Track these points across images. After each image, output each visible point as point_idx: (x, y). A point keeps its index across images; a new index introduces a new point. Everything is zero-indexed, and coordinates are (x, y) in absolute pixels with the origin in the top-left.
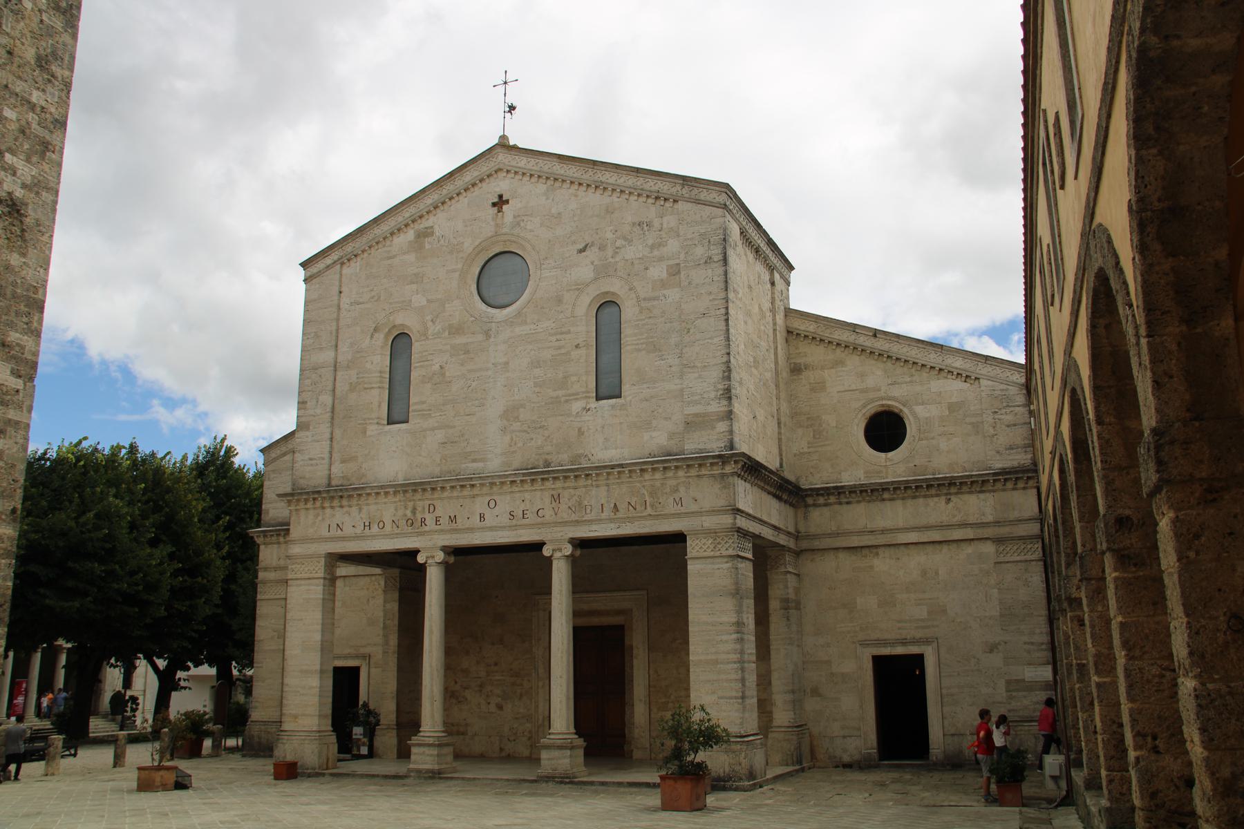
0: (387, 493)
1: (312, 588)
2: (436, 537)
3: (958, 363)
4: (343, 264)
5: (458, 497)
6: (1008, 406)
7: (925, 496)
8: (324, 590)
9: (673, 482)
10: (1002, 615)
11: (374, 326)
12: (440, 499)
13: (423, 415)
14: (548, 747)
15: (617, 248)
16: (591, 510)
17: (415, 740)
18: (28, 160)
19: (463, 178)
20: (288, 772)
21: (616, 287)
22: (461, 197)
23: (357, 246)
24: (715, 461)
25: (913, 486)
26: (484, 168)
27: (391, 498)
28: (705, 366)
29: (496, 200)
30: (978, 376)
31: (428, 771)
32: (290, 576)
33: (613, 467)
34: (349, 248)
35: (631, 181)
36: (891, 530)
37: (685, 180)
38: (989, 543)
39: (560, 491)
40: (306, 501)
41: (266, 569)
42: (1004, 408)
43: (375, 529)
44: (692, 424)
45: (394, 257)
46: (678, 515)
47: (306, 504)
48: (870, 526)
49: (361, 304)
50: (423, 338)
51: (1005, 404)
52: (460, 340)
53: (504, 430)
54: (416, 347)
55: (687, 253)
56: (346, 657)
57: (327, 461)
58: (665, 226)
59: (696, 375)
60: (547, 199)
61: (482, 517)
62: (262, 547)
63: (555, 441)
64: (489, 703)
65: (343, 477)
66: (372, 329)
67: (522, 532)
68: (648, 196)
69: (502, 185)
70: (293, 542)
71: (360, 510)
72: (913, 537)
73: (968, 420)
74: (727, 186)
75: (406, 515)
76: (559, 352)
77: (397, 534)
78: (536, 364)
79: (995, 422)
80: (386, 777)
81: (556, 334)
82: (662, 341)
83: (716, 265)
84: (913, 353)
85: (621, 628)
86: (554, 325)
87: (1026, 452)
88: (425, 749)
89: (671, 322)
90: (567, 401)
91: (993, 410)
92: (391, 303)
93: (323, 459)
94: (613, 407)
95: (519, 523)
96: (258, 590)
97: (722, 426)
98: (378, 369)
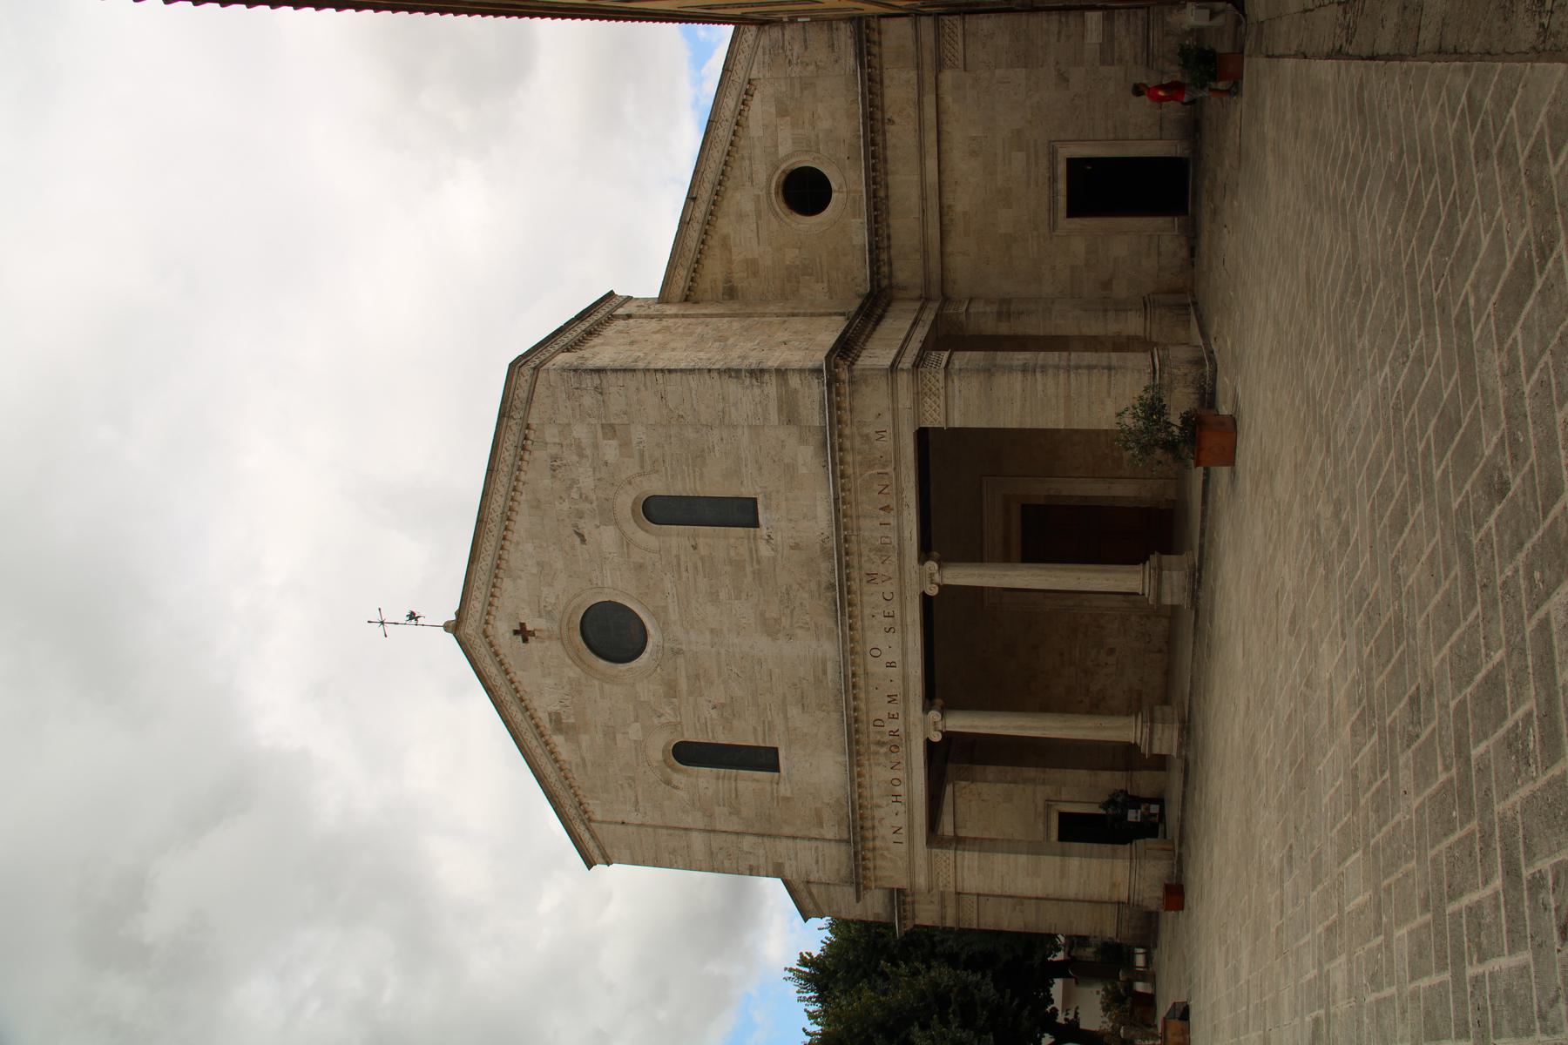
0: (860, 775)
1: (966, 863)
2: (912, 719)
3: (730, 103)
4: (590, 820)
5: (867, 692)
6: (783, 47)
7: (885, 148)
8: (969, 850)
9: (858, 441)
10: (1026, 67)
11: (663, 785)
12: (867, 714)
13: (770, 729)
14: (1159, 596)
15: (581, 497)
16: (887, 537)
17: (1145, 749)
19: (493, 675)
20: (1175, 894)
21: (626, 501)
22: (515, 679)
23: (570, 802)
24: (834, 390)
25: (872, 161)
26: (482, 651)
27: (865, 770)
28: (723, 398)
29: (520, 638)
30: (747, 80)
31: (1181, 735)
32: (953, 889)
33: (837, 510)
34: (572, 812)
35: (502, 480)
36: (922, 189)
37: (503, 414)
38: (942, 77)
39: (863, 573)
40: (865, 868)
41: (943, 918)
42: (784, 51)
43: (900, 789)
44: (790, 417)
45: (583, 759)
46: (896, 436)
47: (869, 869)
49: (637, 799)
50: (679, 729)
51: (781, 51)
52: (683, 685)
53: (790, 637)
54: (690, 736)
55: (589, 415)
56: (1048, 828)
57: (819, 844)
58: (557, 440)
59: (733, 409)
60: (520, 578)
61: (890, 665)
62: (918, 922)
63: (805, 578)
64: (1106, 664)
65: (839, 825)
66: (668, 788)
67: (909, 620)
68: (521, 459)
69: (502, 630)
70: (912, 885)
71: (879, 806)
72: (931, 165)
73: (797, 94)
74: (512, 366)
75: (885, 754)
76: (700, 568)
77: (907, 764)
78: (714, 596)
79: (802, 63)
80: (1185, 783)
81: (679, 572)
82: (692, 448)
83: (604, 381)
84: (717, 155)
86: (668, 573)
87: (837, 29)
88: (1156, 737)
89: (671, 437)
90: (759, 562)
91: (787, 65)
92: (638, 765)
93: (817, 847)
94: (767, 508)
95: (899, 622)
96: (966, 927)
97: (794, 381)
98: (714, 781)
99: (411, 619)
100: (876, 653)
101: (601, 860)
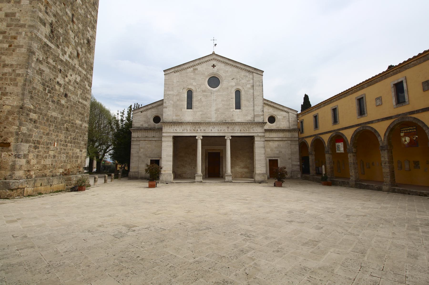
17: (196, 175)
18: (91, 30)
21: (240, 88)
31: (200, 181)
35: (243, 67)
37: (255, 69)
43: (185, 131)
45: (188, 73)
48: (270, 137)
53: (216, 113)
61: (211, 130)
66: (183, 88)
71: (181, 127)
72: (277, 139)
73: (287, 119)
78: (223, 101)
81: (227, 95)
85: (219, 154)
94: (240, 111)
97: (262, 117)
101: (165, 73)
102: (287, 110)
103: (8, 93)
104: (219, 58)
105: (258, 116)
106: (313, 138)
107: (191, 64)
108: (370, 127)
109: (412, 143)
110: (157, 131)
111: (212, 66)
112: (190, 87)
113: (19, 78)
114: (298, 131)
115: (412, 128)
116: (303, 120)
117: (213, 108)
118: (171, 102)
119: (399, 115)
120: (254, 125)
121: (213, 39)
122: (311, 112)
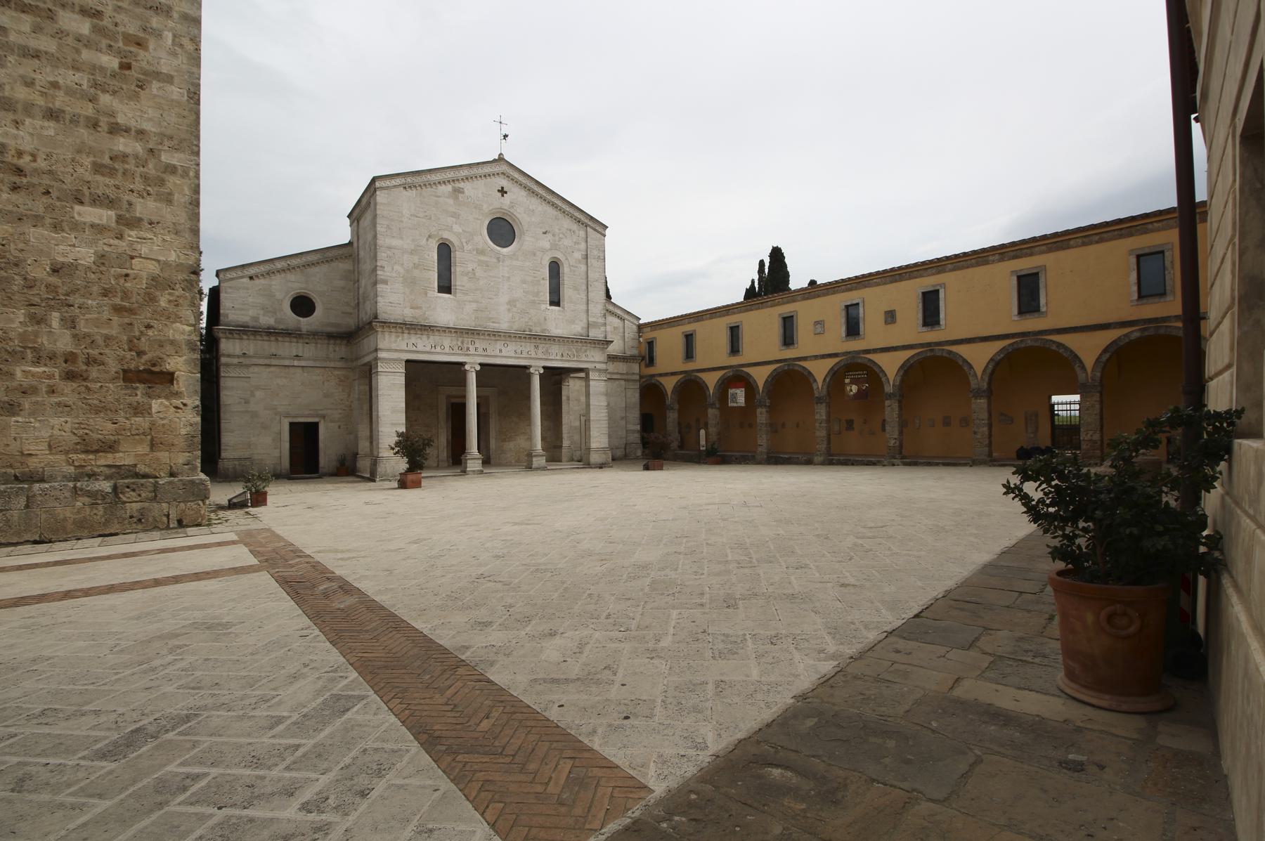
5: (488, 340)
14: (535, 456)
21: (560, 256)
35: (567, 208)
37: (592, 218)
43: (438, 349)
45: (439, 197)
52: (482, 258)
53: (509, 310)
61: (501, 351)
65: (413, 317)
71: (428, 338)
78: (524, 282)
81: (533, 270)
93: (400, 304)
97: (603, 329)
99: (504, 136)
100: (506, 345)
102: (621, 314)
103: (140, 220)
104: (516, 175)
105: (596, 325)
106: (679, 377)
107: (449, 176)
108: (800, 366)
109: (861, 395)
110: (307, 341)
111: (499, 191)
112: (446, 235)
113: (172, 181)
114: (639, 361)
115: (861, 373)
116: (655, 338)
117: (503, 299)
118: (397, 267)
119: (849, 353)
120: (589, 345)
121: (498, 119)
122: (679, 325)
